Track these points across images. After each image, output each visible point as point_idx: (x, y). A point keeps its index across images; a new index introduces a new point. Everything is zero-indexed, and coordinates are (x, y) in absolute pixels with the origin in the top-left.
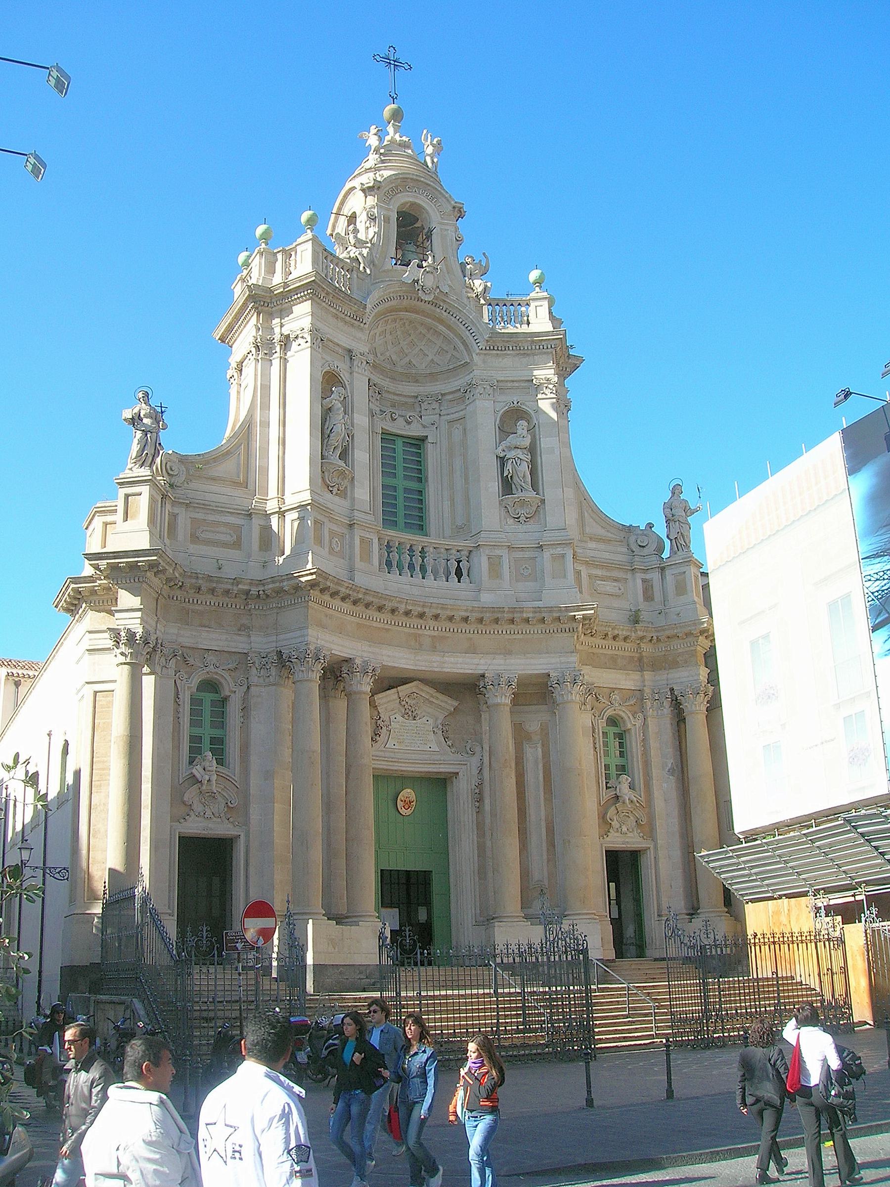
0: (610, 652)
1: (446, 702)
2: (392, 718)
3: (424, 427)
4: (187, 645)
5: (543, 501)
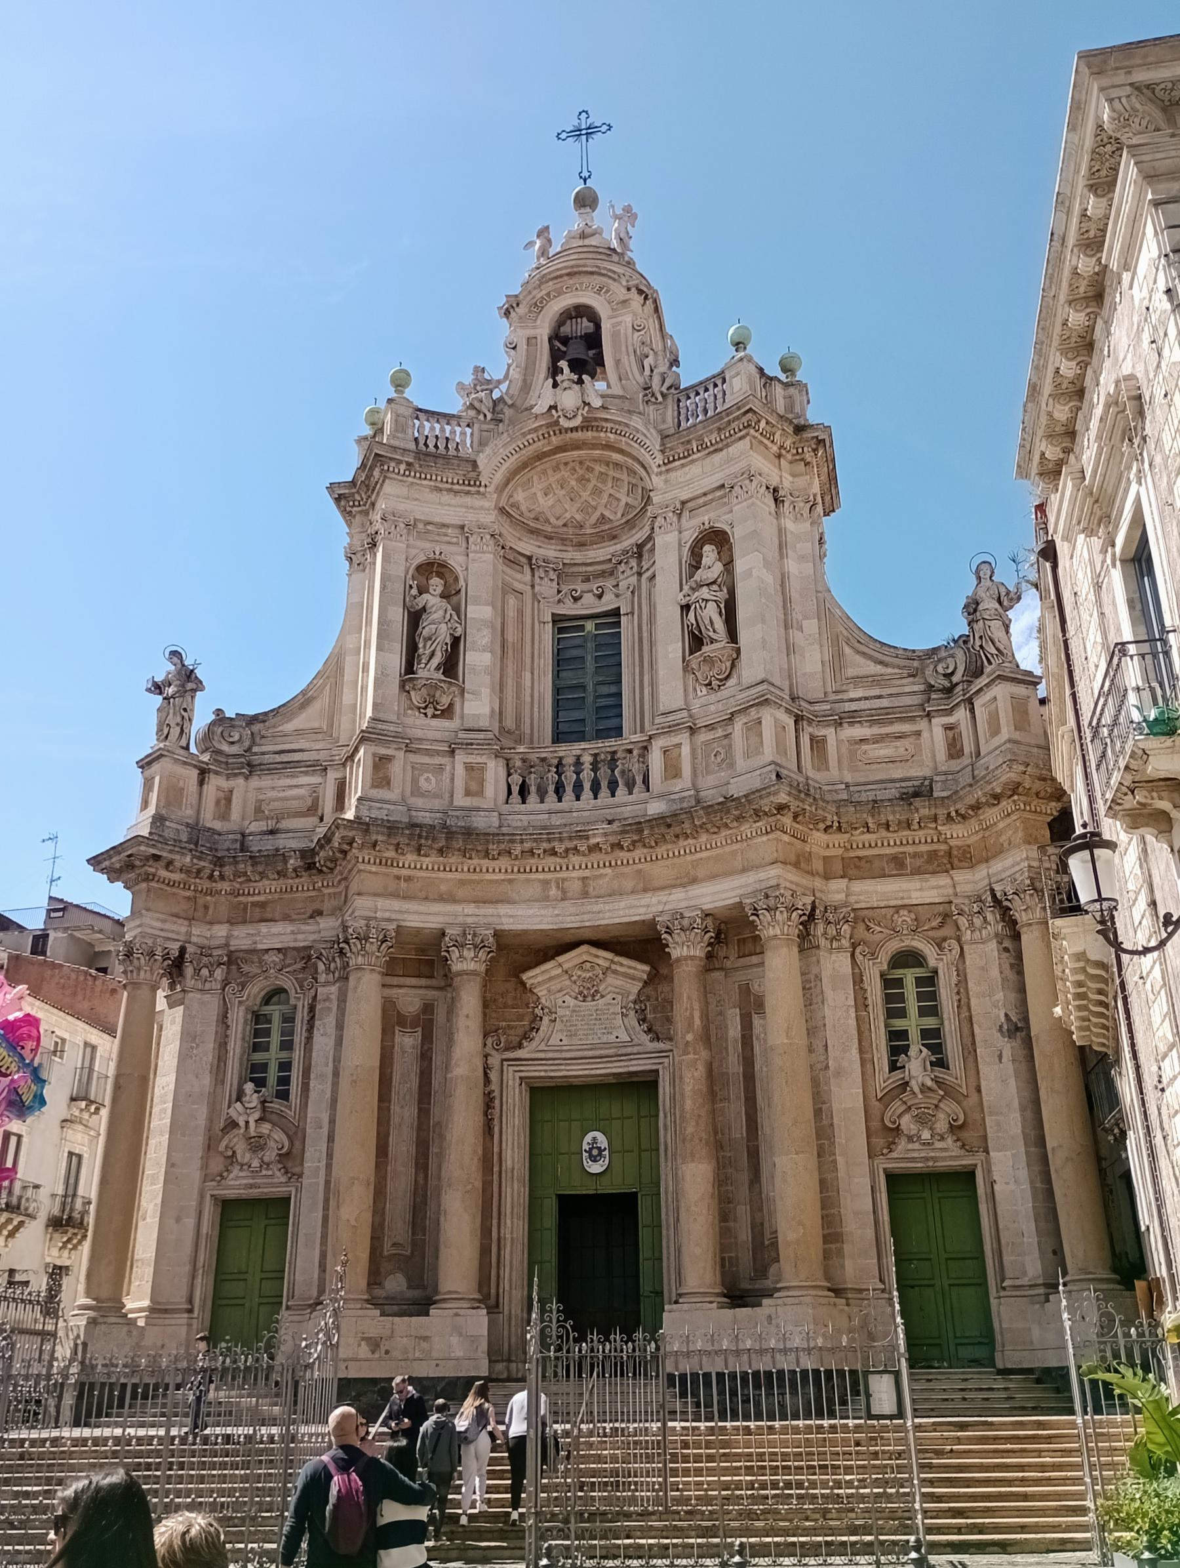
0: (888, 851)
1: (635, 969)
2: (560, 1002)
3: (617, 596)
4: (243, 947)
5: (738, 651)
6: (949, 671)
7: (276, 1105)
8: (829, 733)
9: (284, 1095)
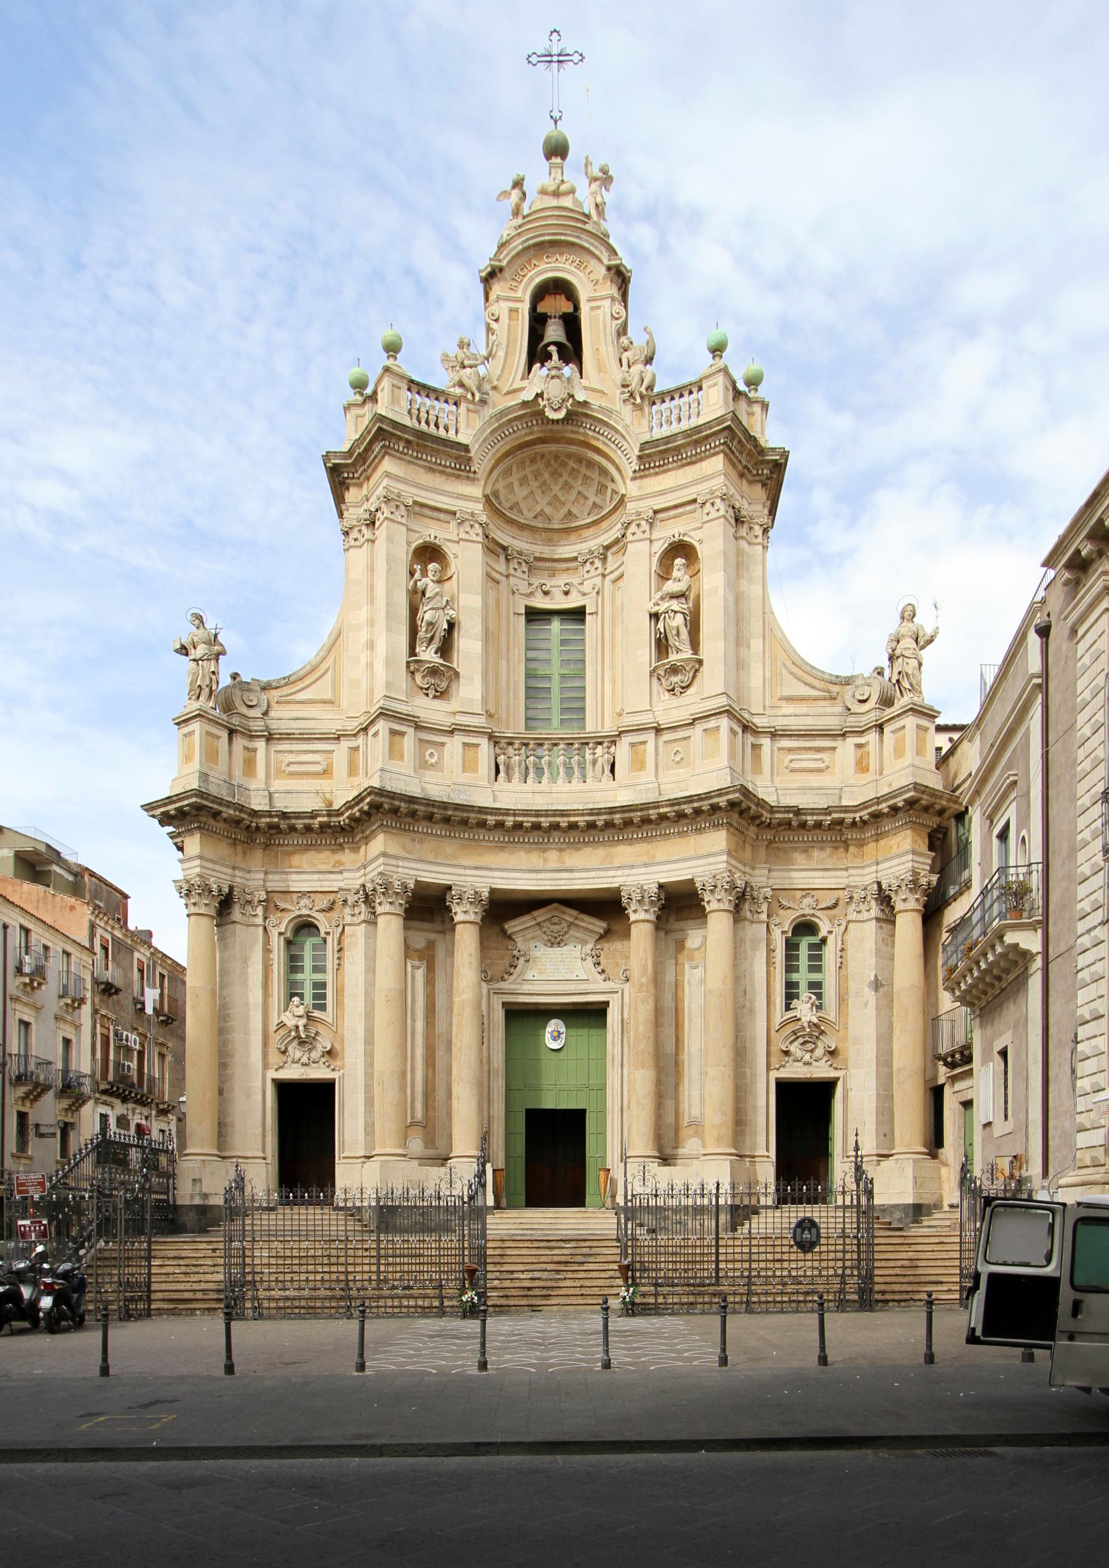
6: (865, 698)
7: (316, 1014)
8: (766, 742)
9: (323, 1007)
